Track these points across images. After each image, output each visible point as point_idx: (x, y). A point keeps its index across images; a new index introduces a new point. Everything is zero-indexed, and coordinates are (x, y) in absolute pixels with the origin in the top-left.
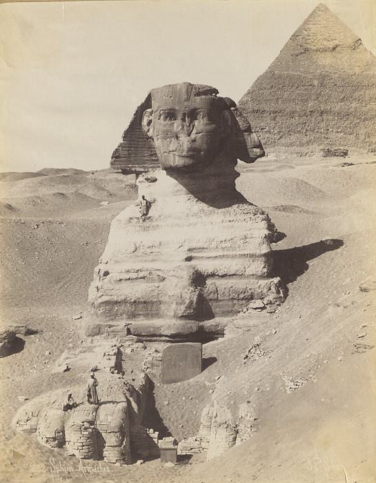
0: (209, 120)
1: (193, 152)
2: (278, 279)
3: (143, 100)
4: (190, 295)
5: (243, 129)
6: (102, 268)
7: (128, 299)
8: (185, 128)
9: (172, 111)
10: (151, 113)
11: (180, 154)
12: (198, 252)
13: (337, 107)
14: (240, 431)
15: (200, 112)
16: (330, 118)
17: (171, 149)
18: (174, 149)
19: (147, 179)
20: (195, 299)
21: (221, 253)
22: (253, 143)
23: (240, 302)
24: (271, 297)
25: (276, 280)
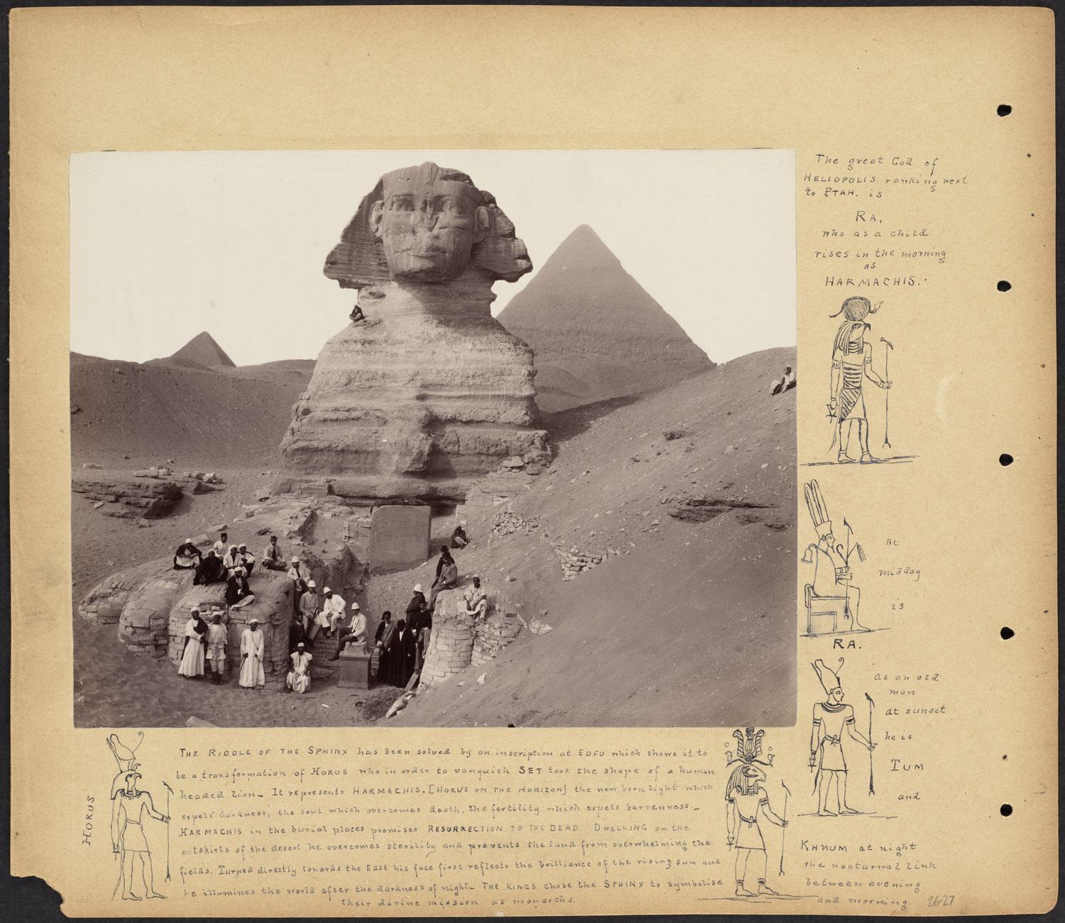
0: (460, 213)
2: (545, 431)
3: (371, 188)
4: (421, 443)
6: (303, 404)
9: (409, 198)
10: (383, 205)
11: (417, 254)
15: (448, 200)
17: (404, 247)
18: (409, 247)
20: (426, 449)
21: (466, 393)
23: (490, 459)
24: (535, 453)
25: (542, 433)
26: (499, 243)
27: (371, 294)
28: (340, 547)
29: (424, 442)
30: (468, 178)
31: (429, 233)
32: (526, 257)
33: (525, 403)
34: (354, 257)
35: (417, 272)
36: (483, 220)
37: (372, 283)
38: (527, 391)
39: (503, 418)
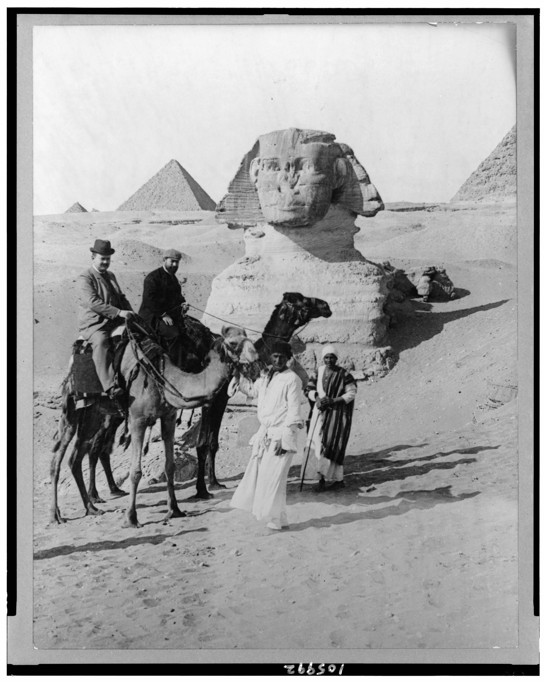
0: (316, 170)
1: (297, 205)
2: (388, 348)
3: (250, 148)
8: (289, 179)
9: (275, 161)
17: (272, 202)
18: (275, 203)
25: (383, 350)
26: (355, 187)
27: (252, 234)
31: (291, 190)
32: (378, 198)
37: (254, 224)
39: (353, 339)
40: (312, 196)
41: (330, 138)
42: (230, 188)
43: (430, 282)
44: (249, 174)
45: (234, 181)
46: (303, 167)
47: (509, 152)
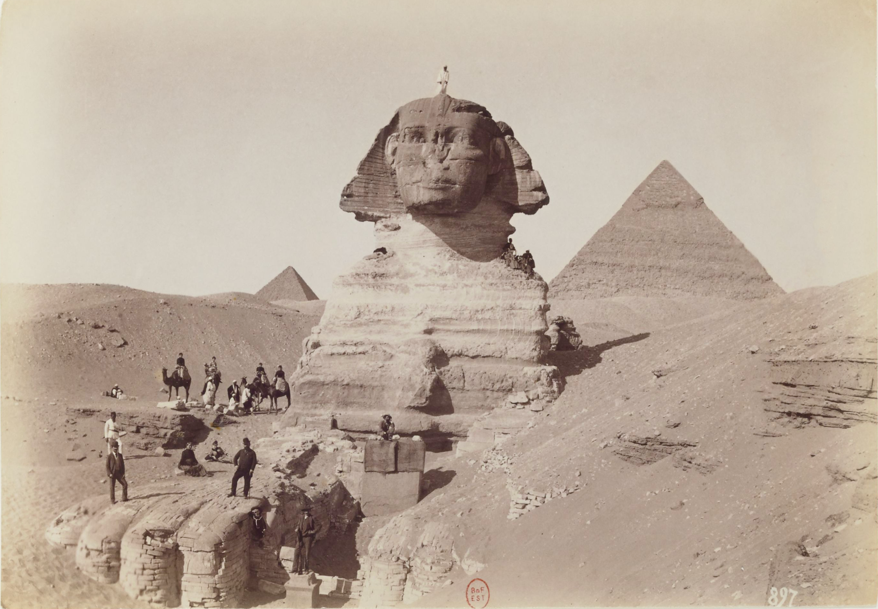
0: (471, 144)
1: (445, 184)
2: (554, 367)
3: (387, 122)
4: (424, 378)
5: (521, 164)
6: (313, 338)
7: (340, 380)
8: (437, 152)
9: (420, 130)
10: (398, 137)
11: (426, 185)
12: (444, 324)
13: (676, 264)
14: (413, 569)
16: (669, 274)
17: (414, 180)
18: (419, 179)
19: (386, 226)
20: (429, 386)
21: (475, 327)
22: (533, 184)
23: (495, 394)
25: (550, 368)
27: (386, 226)
28: (333, 480)
29: (427, 377)
30: (484, 109)
32: (542, 188)
33: (534, 338)
34: (369, 190)
35: (426, 204)
36: (500, 151)
38: (537, 326)
39: (511, 354)
40: (465, 173)
41: (486, 114)
42: (361, 169)
43: (558, 331)
44: (384, 153)
45: (366, 160)
46: (455, 139)
47: (574, 272)
